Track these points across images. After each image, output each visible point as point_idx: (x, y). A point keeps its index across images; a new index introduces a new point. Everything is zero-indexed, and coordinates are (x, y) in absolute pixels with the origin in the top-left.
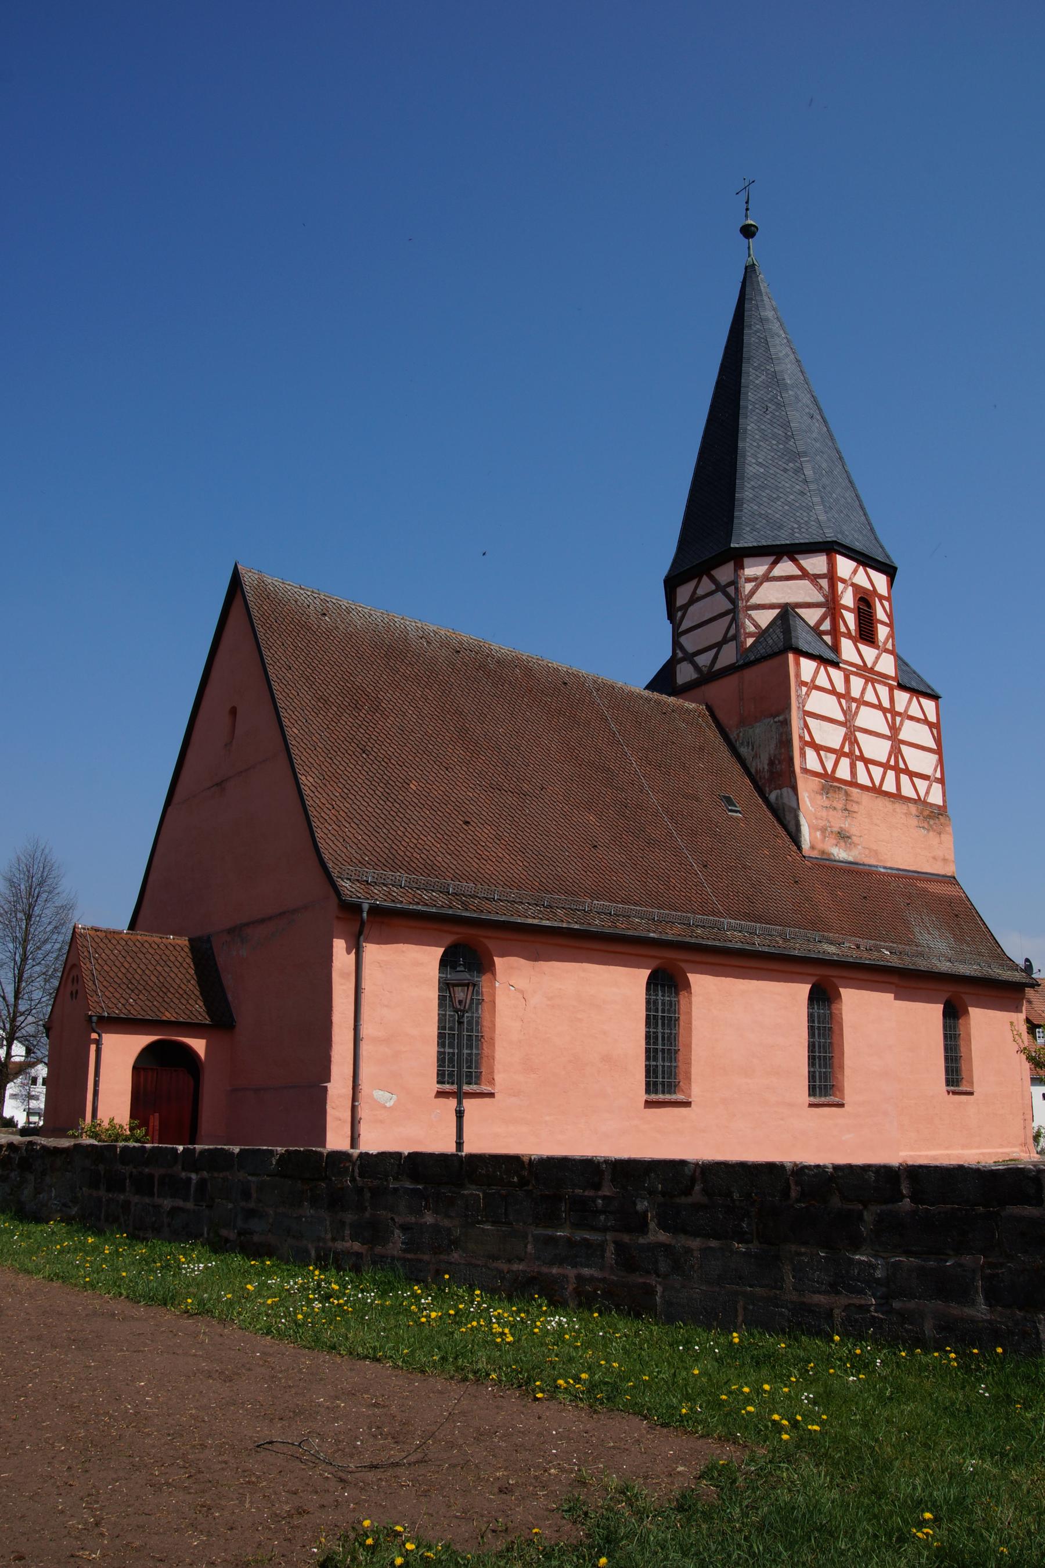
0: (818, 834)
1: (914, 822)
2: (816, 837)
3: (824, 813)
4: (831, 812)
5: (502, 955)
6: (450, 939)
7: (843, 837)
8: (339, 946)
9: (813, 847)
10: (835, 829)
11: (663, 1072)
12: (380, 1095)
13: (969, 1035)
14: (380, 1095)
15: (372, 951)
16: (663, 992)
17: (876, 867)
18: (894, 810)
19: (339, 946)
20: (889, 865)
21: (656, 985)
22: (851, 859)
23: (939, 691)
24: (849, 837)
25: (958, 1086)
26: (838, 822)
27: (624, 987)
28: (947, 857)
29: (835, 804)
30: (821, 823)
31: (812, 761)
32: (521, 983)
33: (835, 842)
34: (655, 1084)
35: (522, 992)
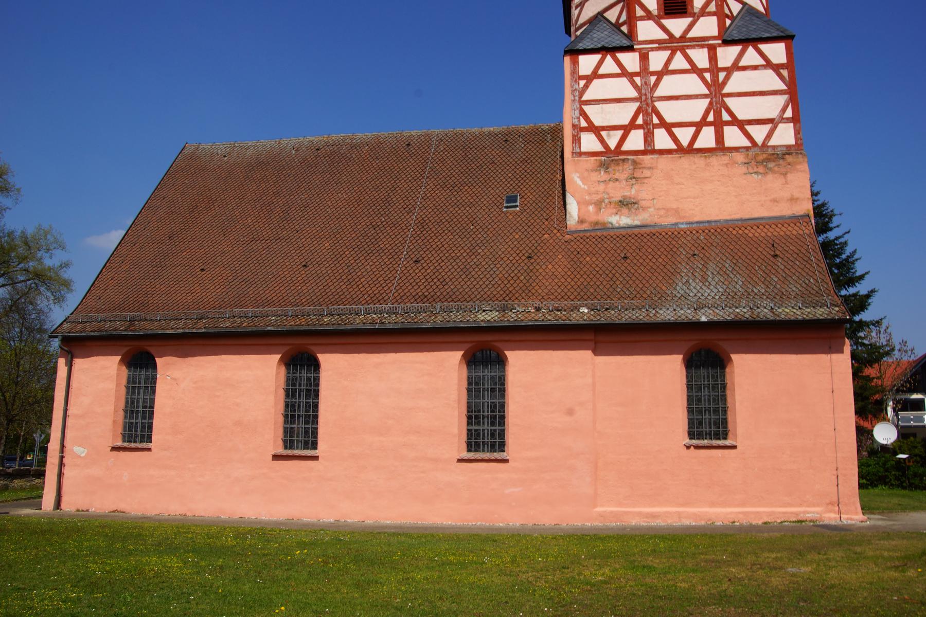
0: (591, 208)
1: (743, 169)
2: (589, 211)
3: (601, 187)
4: (611, 184)
5: (160, 357)
6: (125, 350)
7: (626, 204)
8: (62, 362)
9: (581, 221)
10: (617, 199)
11: (484, 434)
12: (78, 450)
13: (733, 384)
14: (78, 450)
15: (78, 363)
16: (301, 369)
17: (676, 224)
18: (707, 165)
19: (62, 362)
20: (696, 219)
21: (295, 365)
22: (637, 223)
23: (791, 31)
24: (635, 203)
25: (725, 438)
26: (618, 191)
27: (446, 369)
28: (796, 195)
29: (617, 175)
30: (596, 198)
31: (589, 142)
32: (176, 373)
33: (614, 211)
34: (292, 442)
35: (175, 379)
